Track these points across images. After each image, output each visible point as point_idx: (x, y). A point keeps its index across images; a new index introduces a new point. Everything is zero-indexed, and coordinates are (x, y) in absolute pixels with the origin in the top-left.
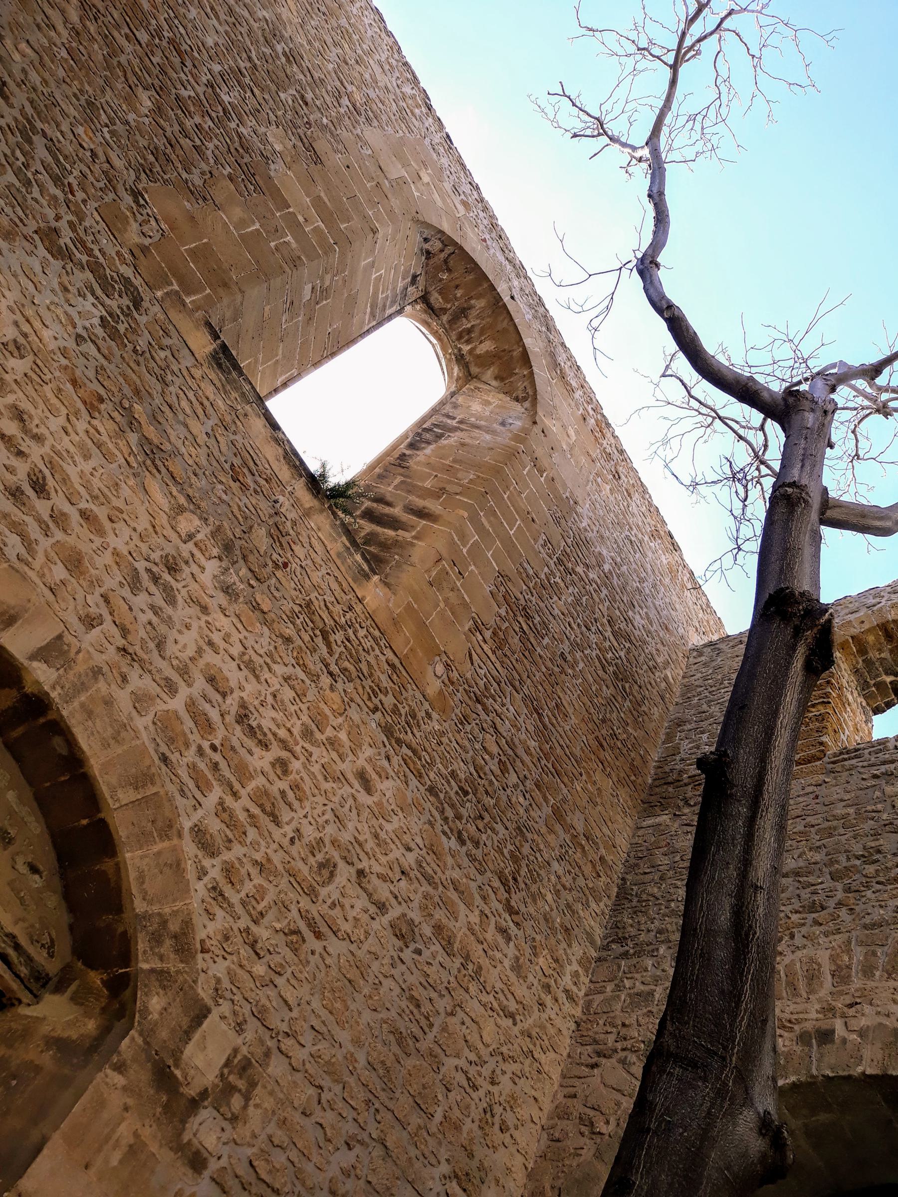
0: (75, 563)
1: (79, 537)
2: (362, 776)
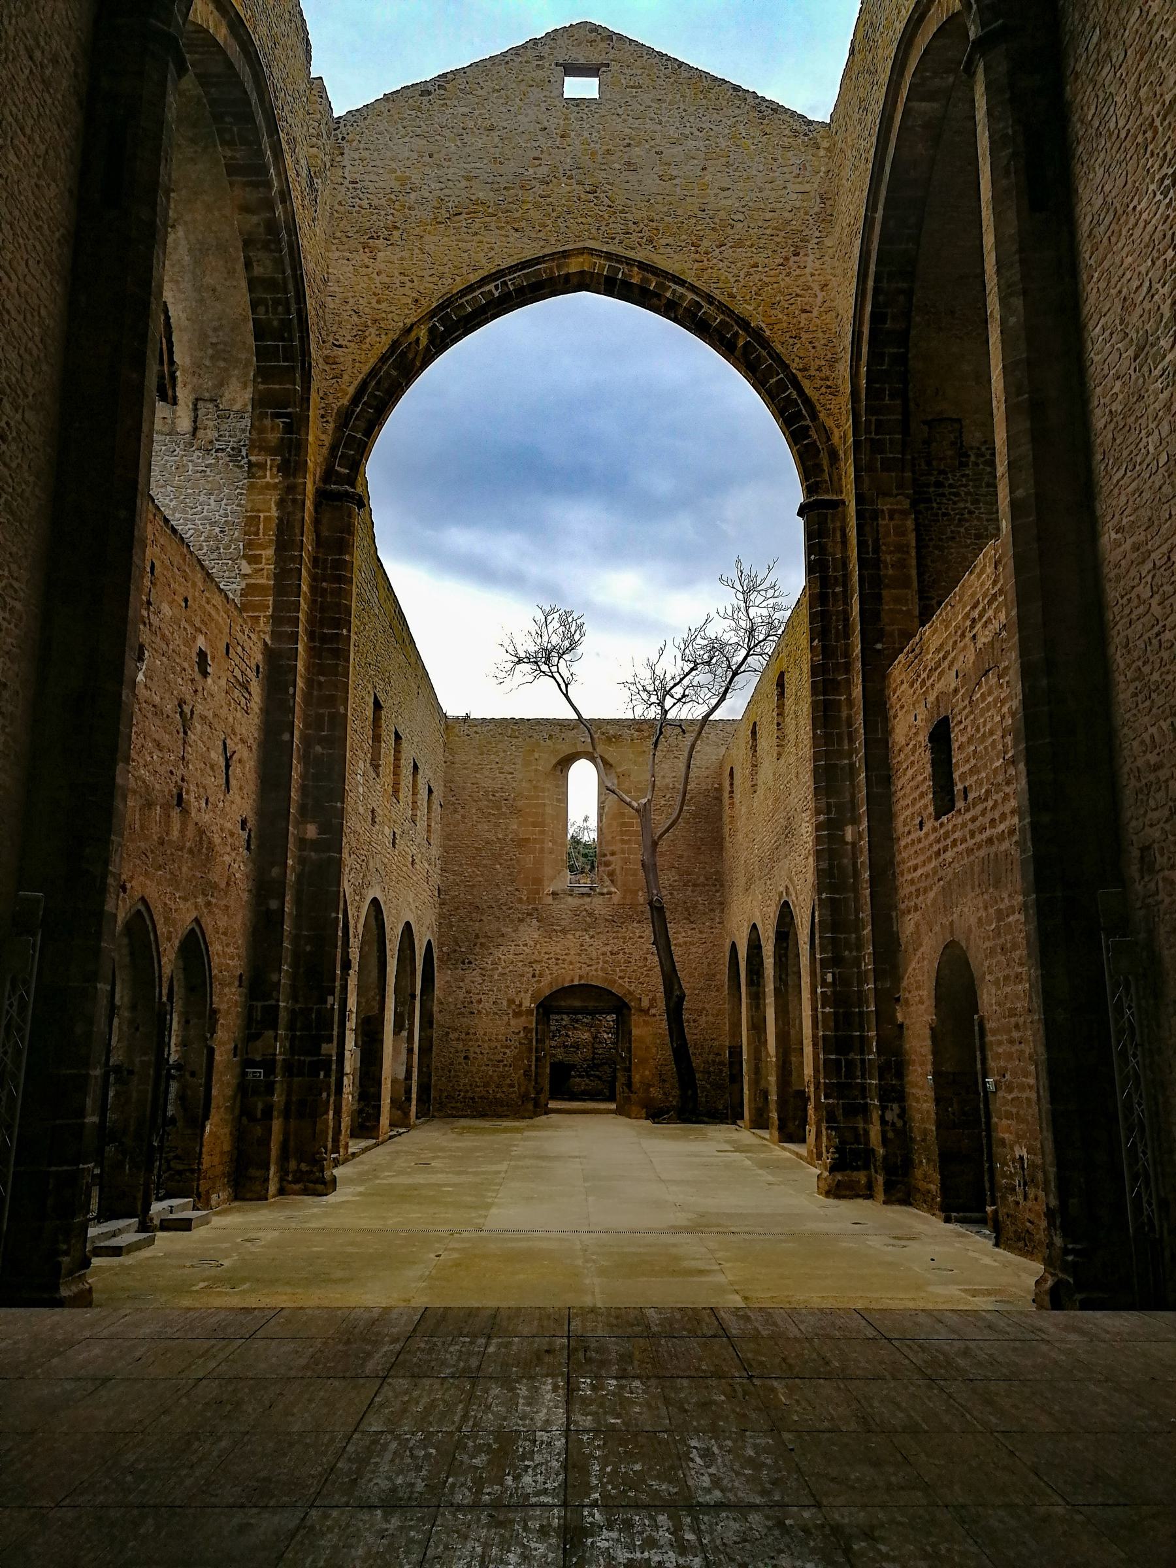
0: (571, 963)
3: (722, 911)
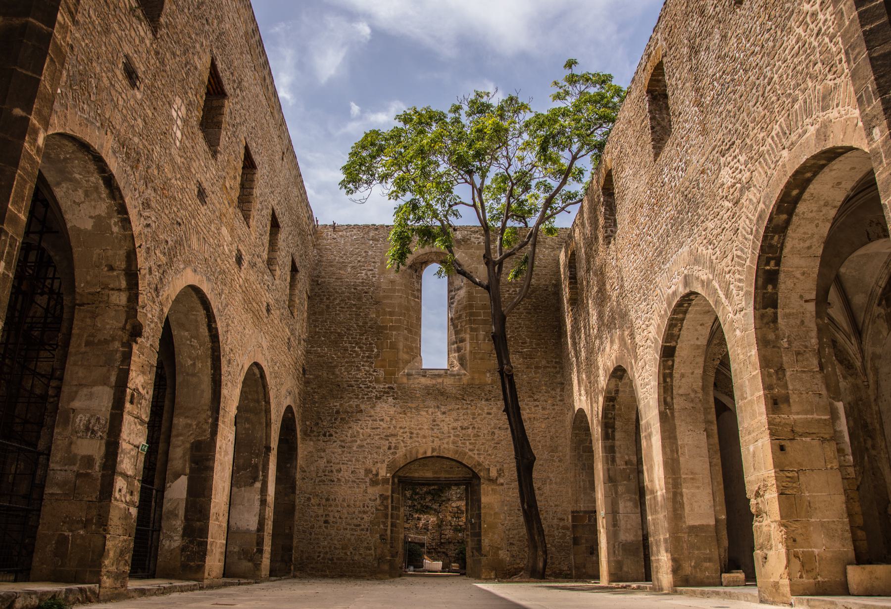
0: (424, 437)
1: (421, 433)
2: (489, 414)
3: (562, 390)
